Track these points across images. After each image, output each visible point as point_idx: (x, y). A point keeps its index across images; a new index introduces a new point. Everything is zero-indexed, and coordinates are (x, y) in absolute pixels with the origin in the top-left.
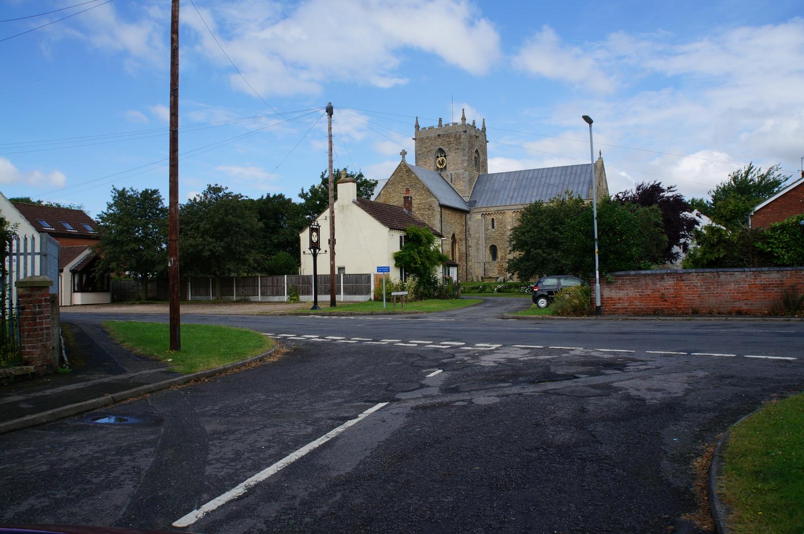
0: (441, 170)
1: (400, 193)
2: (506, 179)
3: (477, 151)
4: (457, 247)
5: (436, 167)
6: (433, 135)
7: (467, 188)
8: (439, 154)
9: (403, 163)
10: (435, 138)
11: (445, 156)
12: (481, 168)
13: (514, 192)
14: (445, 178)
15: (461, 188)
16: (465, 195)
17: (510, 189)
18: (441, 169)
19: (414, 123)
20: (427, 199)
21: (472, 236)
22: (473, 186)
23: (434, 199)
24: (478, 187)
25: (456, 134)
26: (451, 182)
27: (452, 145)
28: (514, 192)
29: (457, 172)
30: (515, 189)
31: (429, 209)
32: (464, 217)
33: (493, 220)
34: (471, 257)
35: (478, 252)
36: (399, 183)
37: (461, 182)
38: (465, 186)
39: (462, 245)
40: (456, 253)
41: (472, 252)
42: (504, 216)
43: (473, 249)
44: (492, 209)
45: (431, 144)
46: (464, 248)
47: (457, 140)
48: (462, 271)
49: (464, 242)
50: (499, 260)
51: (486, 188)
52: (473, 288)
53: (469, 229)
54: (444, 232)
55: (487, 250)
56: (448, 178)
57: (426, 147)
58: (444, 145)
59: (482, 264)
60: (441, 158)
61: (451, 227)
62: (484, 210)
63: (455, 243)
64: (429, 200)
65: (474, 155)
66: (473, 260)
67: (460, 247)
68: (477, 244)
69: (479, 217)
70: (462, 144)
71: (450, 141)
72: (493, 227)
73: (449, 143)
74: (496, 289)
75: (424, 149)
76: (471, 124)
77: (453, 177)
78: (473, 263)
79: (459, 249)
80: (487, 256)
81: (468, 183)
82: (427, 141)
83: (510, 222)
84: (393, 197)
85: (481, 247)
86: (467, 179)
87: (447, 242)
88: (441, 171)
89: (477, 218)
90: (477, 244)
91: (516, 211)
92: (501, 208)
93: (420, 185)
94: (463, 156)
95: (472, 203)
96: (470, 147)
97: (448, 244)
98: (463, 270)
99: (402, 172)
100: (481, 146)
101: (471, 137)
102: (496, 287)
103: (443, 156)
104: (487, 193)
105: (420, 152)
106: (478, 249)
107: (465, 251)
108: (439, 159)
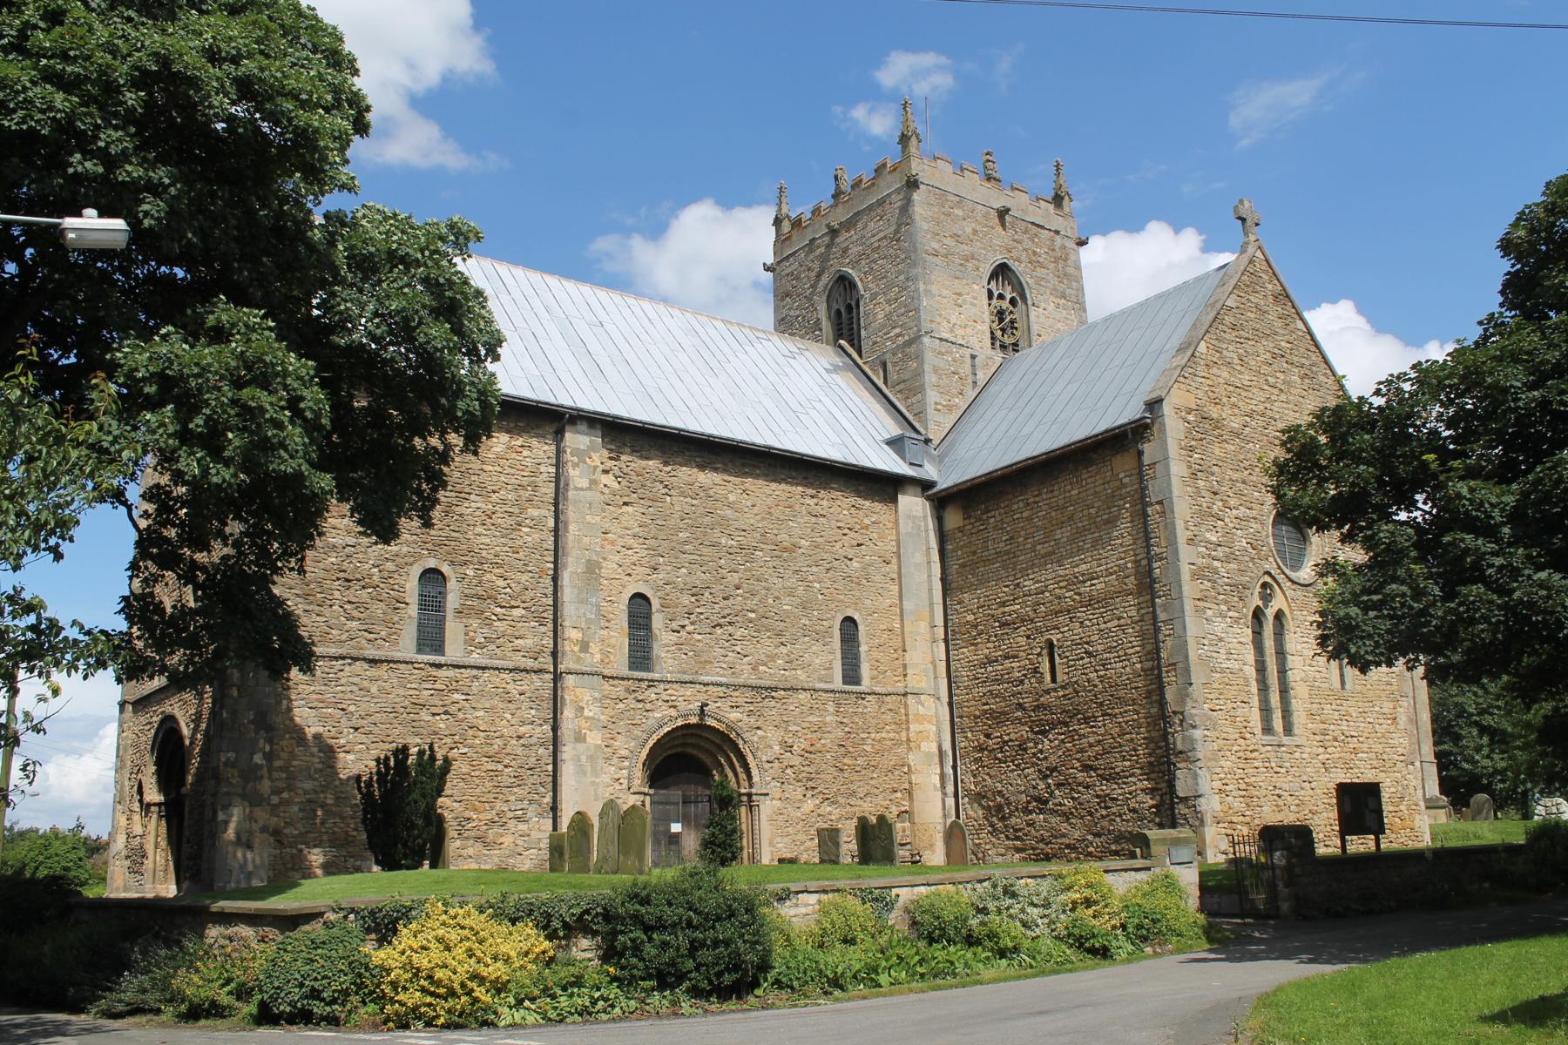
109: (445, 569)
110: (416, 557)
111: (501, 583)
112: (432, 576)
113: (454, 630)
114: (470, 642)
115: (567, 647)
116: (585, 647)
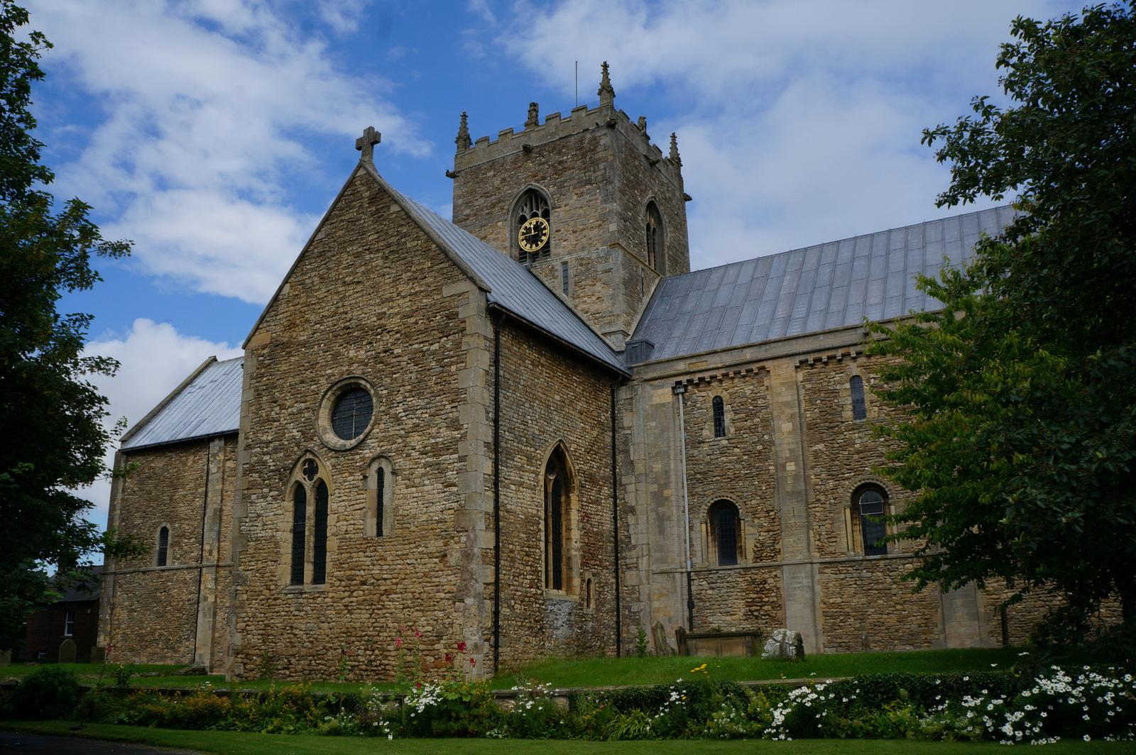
0: (532, 256)
2: (758, 274)
3: (652, 207)
4: (575, 505)
5: (516, 253)
6: (511, 150)
7: (620, 305)
8: (527, 210)
9: (361, 172)
10: (514, 162)
11: (546, 215)
12: (667, 264)
13: (792, 305)
15: (596, 306)
16: (613, 329)
17: (777, 298)
18: (534, 256)
19: (455, 132)
21: (640, 468)
23: (465, 286)
24: (660, 309)
25: (581, 141)
26: (566, 291)
27: (568, 173)
28: (792, 305)
29: (583, 254)
30: (793, 297)
32: (605, 395)
33: (718, 405)
34: (634, 553)
35: (662, 531)
36: (343, 245)
37: (599, 287)
38: (613, 297)
39: (597, 502)
40: (569, 530)
41: (640, 530)
42: (761, 382)
43: (643, 519)
45: (504, 180)
46: (608, 517)
47: (584, 156)
48: (598, 610)
50: (747, 560)
51: (689, 307)
52: (625, 702)
53: (626, 443)
54: (511, 430)
55: (697, 523)
56: (554, 277)
57: (486, 195)
58: (544, 178)
59: (681, 580)
60: (534, 221)
61: (549, 420)
62: (681, 366)
63: (568, 491)
64: (447, 291)
65: (643, 218)
66: (643, 563)
67: (592, 509)
69: (663, 394)
70: (601, 166)
71: (561, 163)
72: (720, 430)
73: (560, 168)
74: (779, 716)
75: (482, 200)
76: (635, 120)
77: (571, 272)
78: (643, 574)
79: (585, 517)
80: (698, 548)
81: (622, 290)
82: (492, 173)
83: (787, 404)
84: (320, 301)
85: (674, 509)
86: (620, 274)
87: (528, 478)
88: (534, 261)
89: (657, 400)
91: (811, 358)
92: (748, 355)
93: (418, 238)
94: (605, 201)
95: (640, 348)
96: (627, 179)
97: (533, 489)
98: (601, 603)
99: (357, 204)
100: (669, 200)
101: (632, 152)
102: (777, 695)
103: (540, 213)
104: (690, 322)
105: (467, 211)
106: (661, 520)
107: (608, 526)
108: (527, 224)
109: (168, 526)
110: (161, 522)
111: (187, 528)
112: (164, 531)
114: (175, 558)
115: (206, 554)
116: (211, 553)
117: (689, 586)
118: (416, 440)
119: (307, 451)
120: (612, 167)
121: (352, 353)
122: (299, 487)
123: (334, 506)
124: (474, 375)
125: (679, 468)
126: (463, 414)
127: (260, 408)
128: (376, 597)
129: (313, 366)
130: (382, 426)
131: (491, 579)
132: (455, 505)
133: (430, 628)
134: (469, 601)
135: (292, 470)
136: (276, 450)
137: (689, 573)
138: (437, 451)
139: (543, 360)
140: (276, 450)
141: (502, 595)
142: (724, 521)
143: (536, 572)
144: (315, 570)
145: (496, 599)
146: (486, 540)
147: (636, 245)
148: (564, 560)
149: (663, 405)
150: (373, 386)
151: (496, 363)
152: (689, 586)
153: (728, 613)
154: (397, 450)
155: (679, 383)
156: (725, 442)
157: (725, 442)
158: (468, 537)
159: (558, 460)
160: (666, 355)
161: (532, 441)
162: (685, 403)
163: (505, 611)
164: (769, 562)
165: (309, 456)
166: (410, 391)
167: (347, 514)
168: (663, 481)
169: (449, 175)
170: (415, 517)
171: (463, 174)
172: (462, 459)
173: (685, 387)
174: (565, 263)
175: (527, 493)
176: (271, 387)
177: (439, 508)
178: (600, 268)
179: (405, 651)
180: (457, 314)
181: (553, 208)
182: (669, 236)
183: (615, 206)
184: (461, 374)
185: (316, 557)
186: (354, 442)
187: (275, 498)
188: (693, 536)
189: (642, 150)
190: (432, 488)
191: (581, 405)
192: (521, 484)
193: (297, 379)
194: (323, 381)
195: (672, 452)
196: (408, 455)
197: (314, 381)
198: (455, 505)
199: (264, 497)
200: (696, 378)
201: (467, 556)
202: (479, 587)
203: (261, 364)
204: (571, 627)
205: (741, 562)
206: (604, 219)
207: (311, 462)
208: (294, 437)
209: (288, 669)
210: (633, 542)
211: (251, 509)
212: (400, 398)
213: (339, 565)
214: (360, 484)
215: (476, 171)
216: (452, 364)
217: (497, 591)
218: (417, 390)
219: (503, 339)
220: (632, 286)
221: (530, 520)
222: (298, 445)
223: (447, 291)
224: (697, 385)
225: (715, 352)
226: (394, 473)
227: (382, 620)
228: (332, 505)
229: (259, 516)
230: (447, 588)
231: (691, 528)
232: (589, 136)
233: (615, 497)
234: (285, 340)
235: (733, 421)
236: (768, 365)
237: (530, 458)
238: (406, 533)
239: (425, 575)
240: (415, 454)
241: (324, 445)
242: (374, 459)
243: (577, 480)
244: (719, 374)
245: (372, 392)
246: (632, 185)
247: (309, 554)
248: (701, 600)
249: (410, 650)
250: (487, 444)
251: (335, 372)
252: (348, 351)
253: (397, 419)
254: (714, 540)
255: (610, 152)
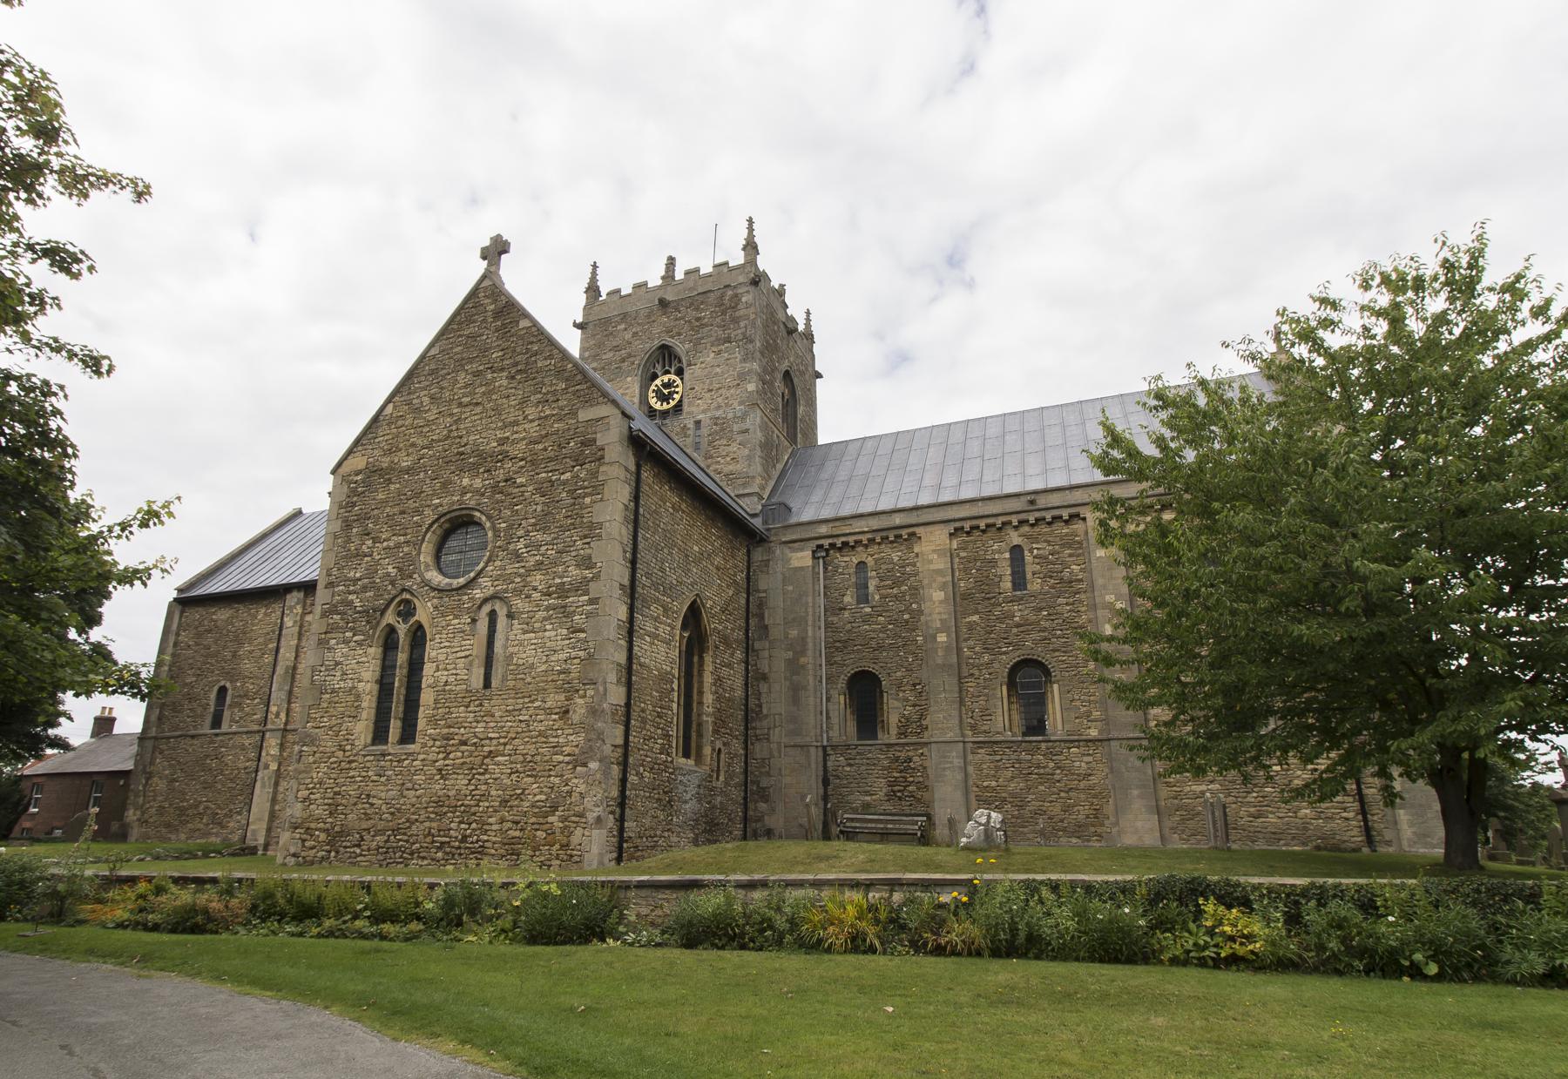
1: (460, 405)
4: (709, 667)
7: (757, 468)
10: (648, 316)
11: (680, 373)
14: (675, 438)
18: (665, 414)
20: (574, 414)
21: (775, 633)
22: (775, 474)
25: (722, 296)
29: (718, 413)
31: (579, 461)
37: (734, 447)
38: (750, 458)
39: (729, 666)
40: (701, 693)
41: (775, 700)
43: (776, 687)
44: (859, 526)
46: (739, 682)
47: (724, 313)
49: (739, 655)
50: (890, 735)
53: (761, 605)
54: (648, 576)
55: (834, 693)
57: (616, 348)
58: (679, 334)
59: (815, 755)
60: (666, 378)
61: (687, 571)
62: (823, 530)
63: (702, 650)
64: (583, 415)
65: (779, 385)
66: (776, 735)
68: (794, 667)
69: (802, 558)
71: (698, 319)
77: (704, 431)
79: (718, 680)
80: (835, 720)
81: (758, 452)
85: (811, 679)
89: (795, 563)
90: (794, 667)
93: (551, 357)
94: (744, 360)
97: (668, 643)
101: (772, 314)
107: (739, 693)
113: (227, 714)
117: (825, 761)
118: (537, 579)
119: (403, 590)
120: (753, 323)
121: (466, 482)
122: (391, 630)
123: (433, 654)
124: (611, 510)
125: (816, 635)
126: (598, 551)
127: (349, 541)
128: (478, 760)
129: (417, 495)
130: (498, 563)
131: (620, 741)
132: (581, 654)
133: (543, 797)
134: (593, 765)
135: (383, 612)
136: (365, 589)
137: (824, 748)
138: (562, 591)
139: (684, 506)
140: (365, 589)
141: (631, 760)
142: (865, 693)
143: (667, 736)
144: (404, 729)
145: (624, 765)
146: (617, 695)
147: (772, 410)
148: (694, 726)
149: (802, 568)
150: (489, 517)
151: (636, 498)
152: (825, 761)
153: (867, 793)
154: (515, 590)
155: (820, 547)
156: (868, 610)
157: (868, 610)
158: (597, 690)
159: (694, 615)
160: (805, 518)
161: (669, 590)
162: (825, 569)
163: (632, 778)
164: (914, 739)
165: (406, 596)
166: (534, 525)
167: (448, 662)
168: (799, 648)
169: (576, 325)
170: (532, 666)
171: (591, 326)
172: (592, 601)
173: (827, 551)
174: (698, 423)
175: (662, 648)
176: (363, 518)
177: (563, 656)
178: (736, 428)
179: (509, 825)
180: (595, 440)
181: (689, 365)
182: (801, 410)
183: (755, 366)
184: (597, 506)
185: (405, 712)
186: (462, 581)
187: (360, 644)
188: (831, 707)
189: (781, 316)
190: (555, 634)
191: (718, 560)
192: (655, 636)
193: (396, 510)
194: (427, 511)
195: (810, 618)
196: (528, 596)
197: (417, 511)
198: (581, 654)
199: (346, 642)
200: (839, 542)
201: (593, 712)
202: (607, 749)
203: (354, 492)
204: (699, 801)
205: (883, 738)
206: (742, 377)
207: (408, 602)
208: (388, 574)
209: (359, 846)
210: (765, 711)
211: (329, 655)
212: (521, 533)
213: (433, 721)
214: (467, 628)
215: (605, 323)
216: (586, 495)
217: (626, 755)
218: (542, 524)
219: (644, 475)
220: (768, 447)
221: (664, 678)
222: (393, 583)
223: (583, 415)
224: (840, 549)
225: (861, 516)
226: (510, 616)
227: (484, 787)
228: (431, 651)
229: (337, 664)
230: (567, 750)
231: (828, 700)
232: (730, 292)
233: (747, 663)
234: (385, 465)
235: (878, 588)
236: (917, 530)
237: (666, 610)
238: (520, 684)
239: (541, 734)
240: (536, 595)
241: (425, 583)
242: (486, 601)
243: (713, 640)
244: (864, 538)
245: (488, 525)
246: (770, 349)
247: (397, 707)
248: (838, 777)
249: (517, 823)
250: (622, 586)
251: (447, 502)
252: (461, 479)
253: (517, 556)
254: (852, 713)
255: (752, 310)
